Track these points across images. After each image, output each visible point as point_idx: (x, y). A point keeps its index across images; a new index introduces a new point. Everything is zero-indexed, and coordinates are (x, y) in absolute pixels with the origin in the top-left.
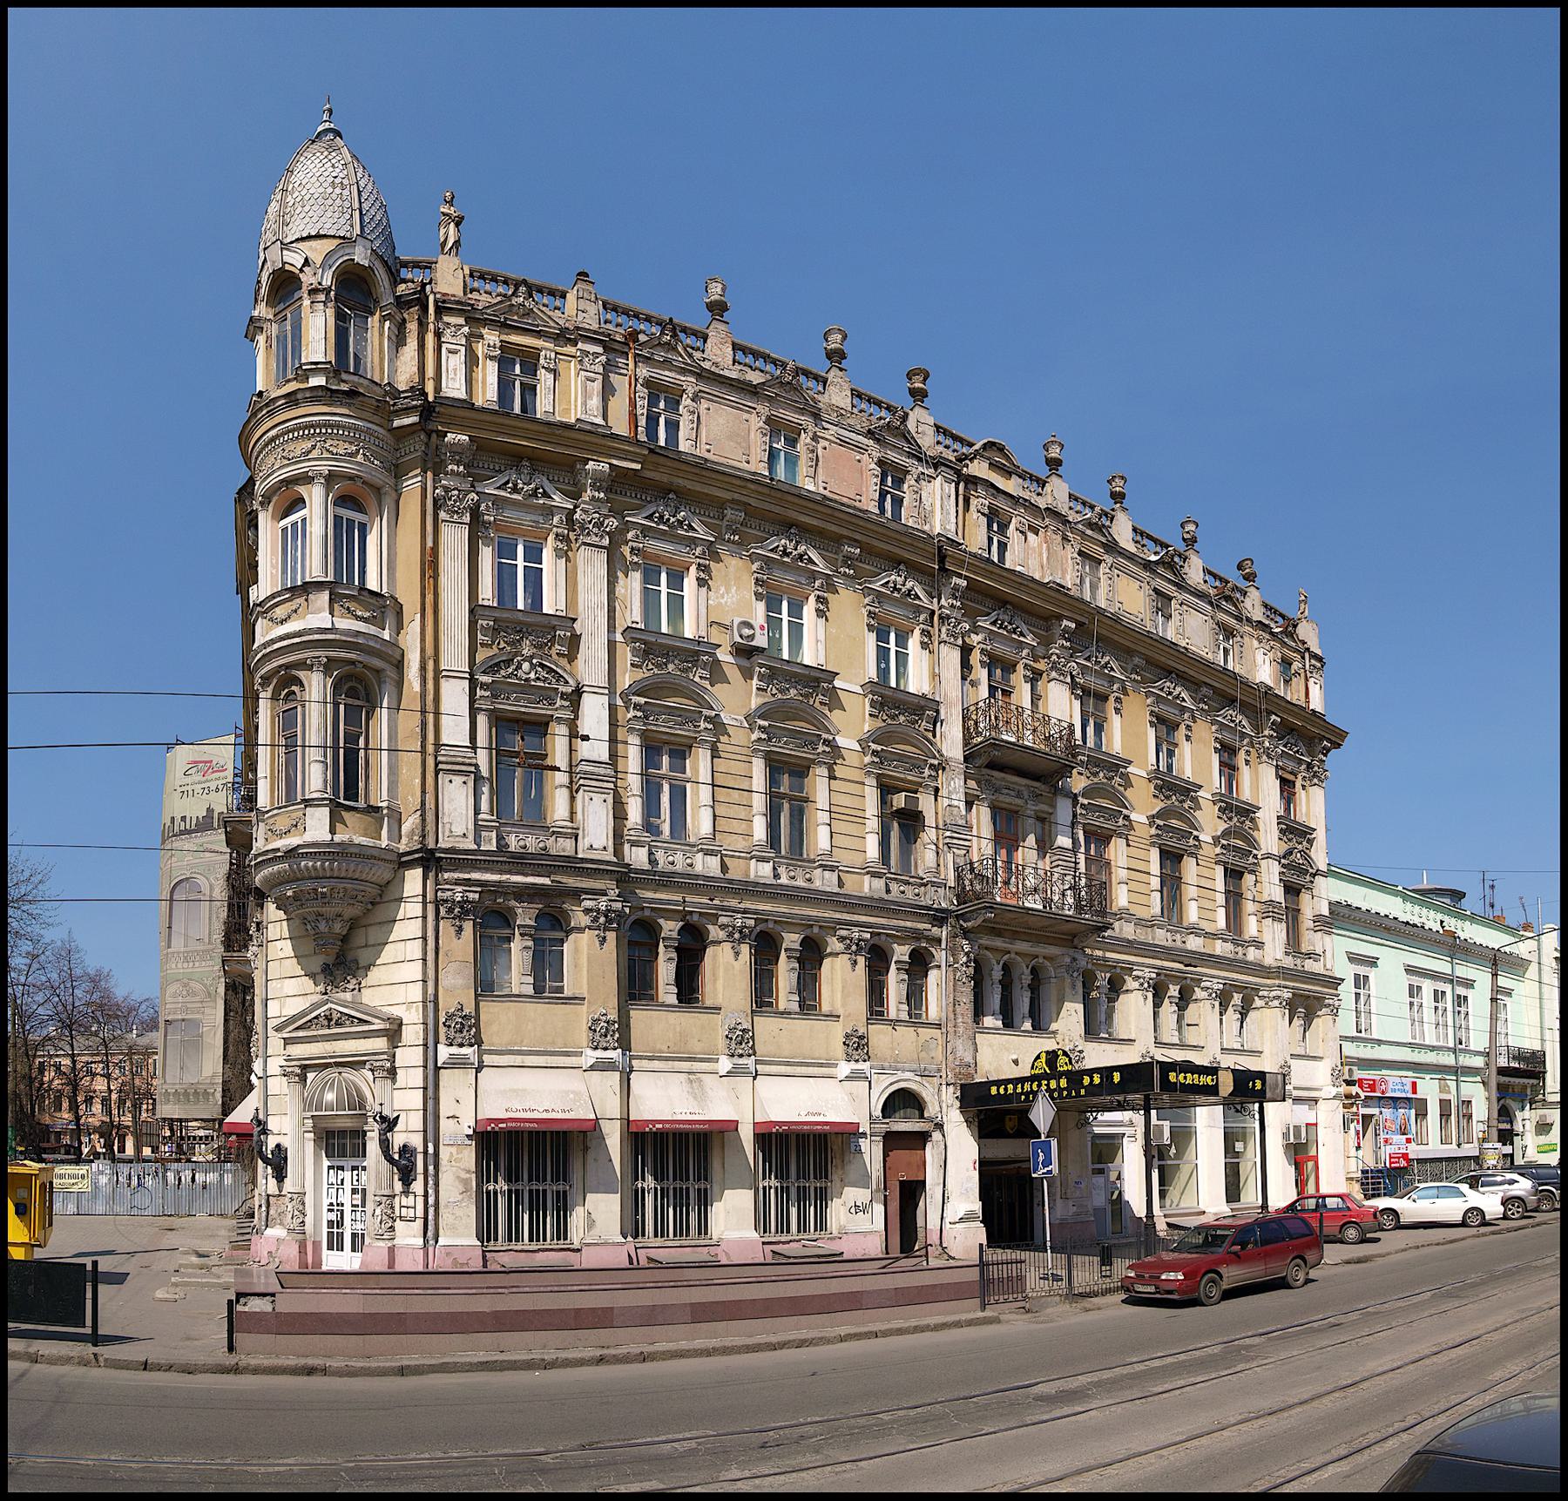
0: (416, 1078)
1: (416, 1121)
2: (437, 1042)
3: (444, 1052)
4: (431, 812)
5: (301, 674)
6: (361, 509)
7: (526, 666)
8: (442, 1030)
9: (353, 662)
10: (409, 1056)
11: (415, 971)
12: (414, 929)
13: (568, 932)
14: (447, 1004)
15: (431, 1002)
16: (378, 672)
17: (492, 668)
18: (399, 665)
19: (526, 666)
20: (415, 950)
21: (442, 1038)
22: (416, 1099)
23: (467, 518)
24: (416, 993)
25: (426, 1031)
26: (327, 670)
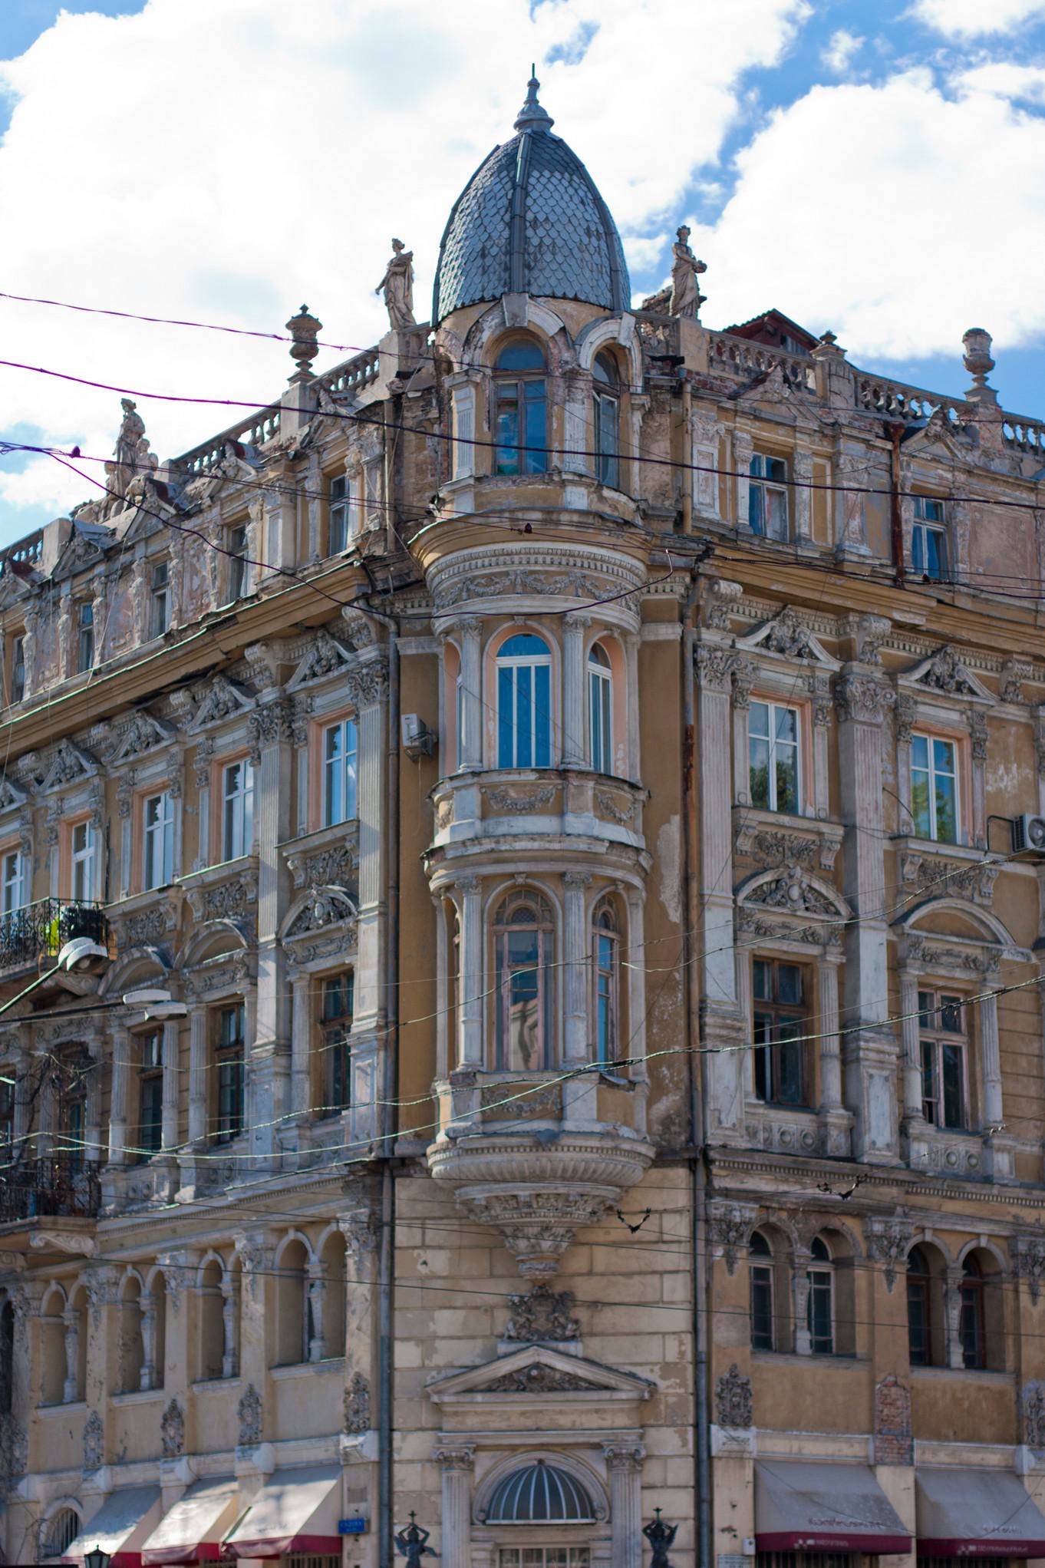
0: (683, 1471)
1: (684, 1536)
2: (710, 1422)
3: (719, 1436)
4: (695, 1094)
5: (549, 889)
6: (607, 666)
7: (795, 893)
8: (715, 1401)
9: (613, 881)
10: (671, 1443)
11: (680, 1320)
12: (676, 1258)
13: (844, 1264)
14: (720, 1368)
15: (701, 1362)
16: (629, 887)
17: (761, 896)
18: (651, 879)
19: (795, 893)
20: (678, 1288)
21: (715, 1415)
22: (678, 1506)
23: (728, 687)
24: (678, 1350)
25: (697, 1404)
26: (588, 888)
